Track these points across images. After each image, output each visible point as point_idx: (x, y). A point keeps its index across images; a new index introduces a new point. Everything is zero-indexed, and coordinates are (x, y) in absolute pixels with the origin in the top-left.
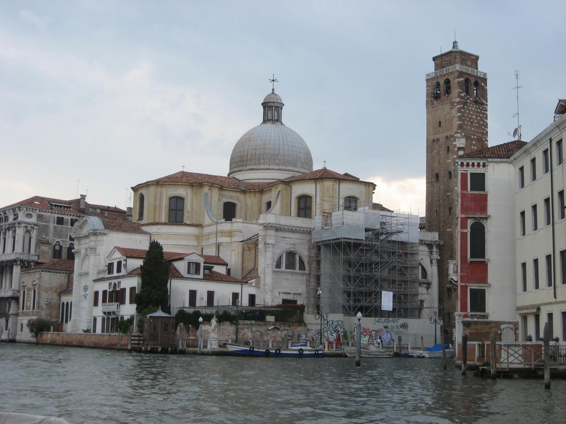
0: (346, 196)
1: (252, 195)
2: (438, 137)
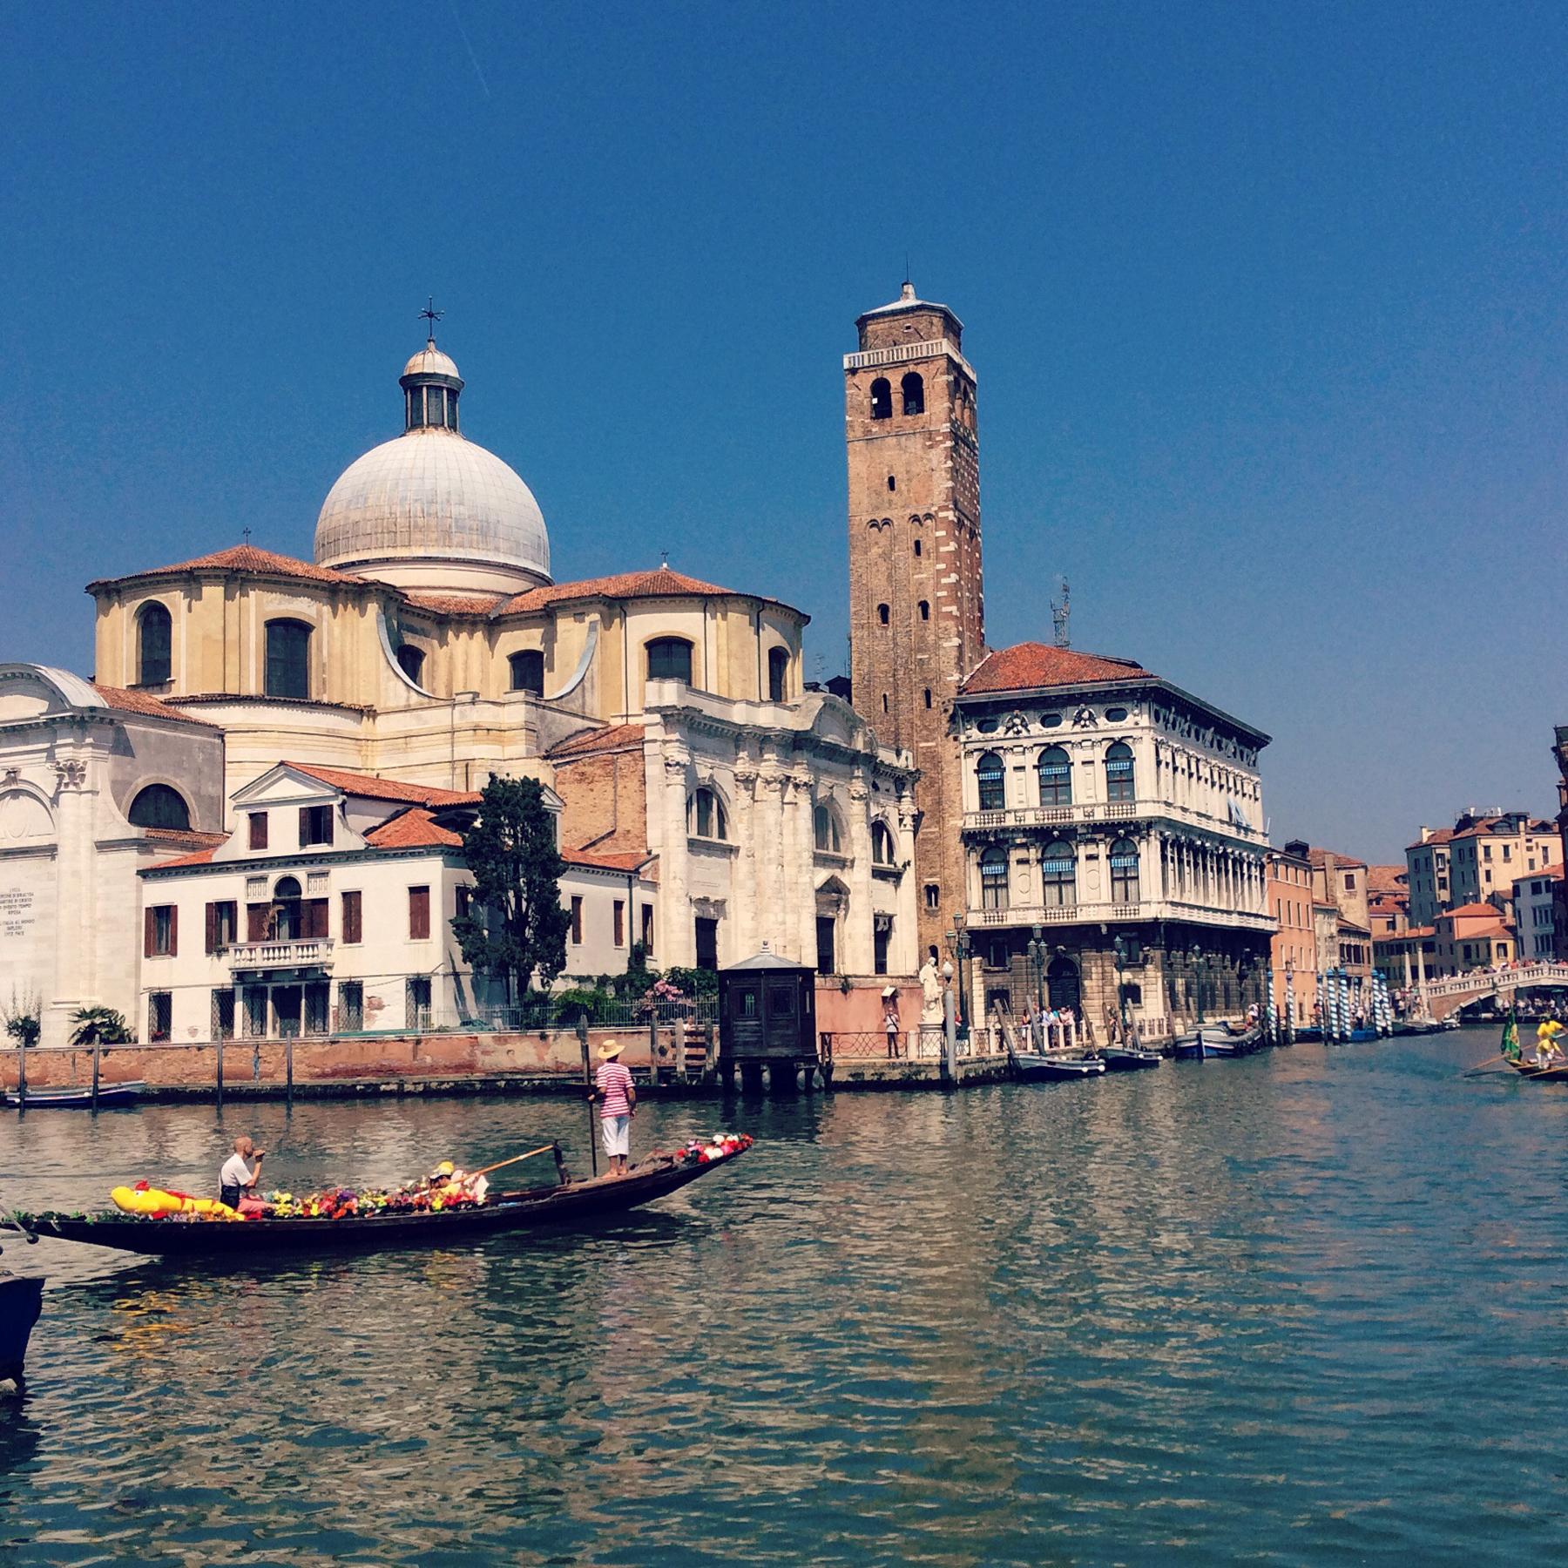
1: (464, 636)
2: (888, 516)
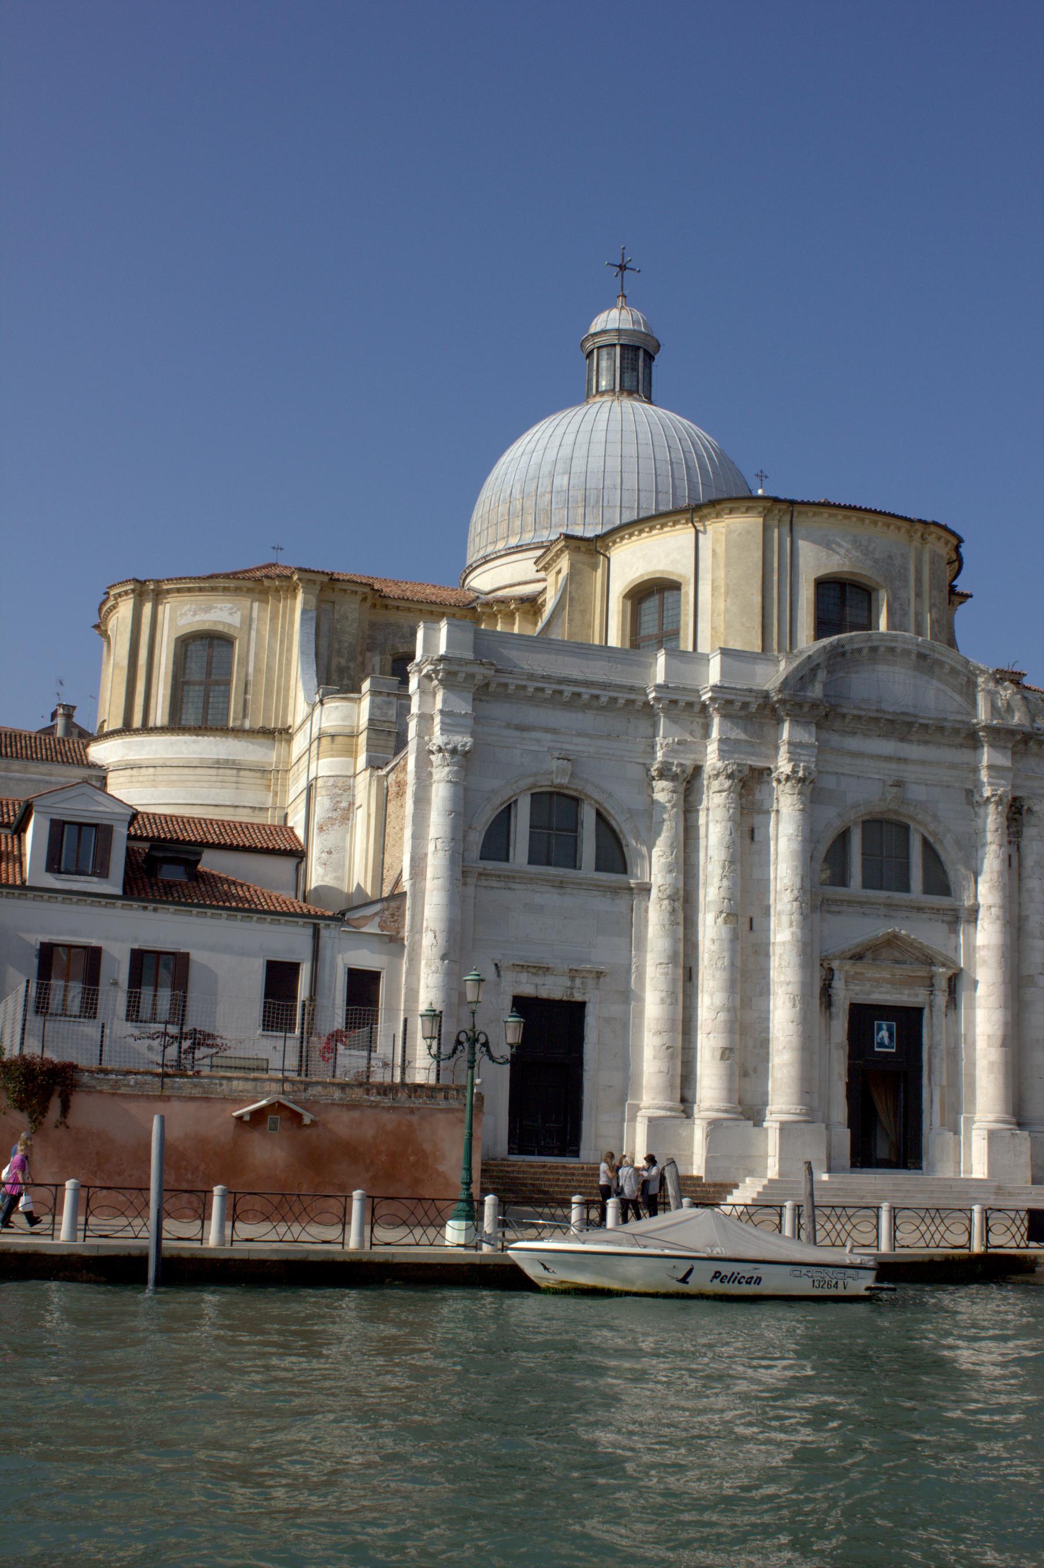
0: (822, 572)
